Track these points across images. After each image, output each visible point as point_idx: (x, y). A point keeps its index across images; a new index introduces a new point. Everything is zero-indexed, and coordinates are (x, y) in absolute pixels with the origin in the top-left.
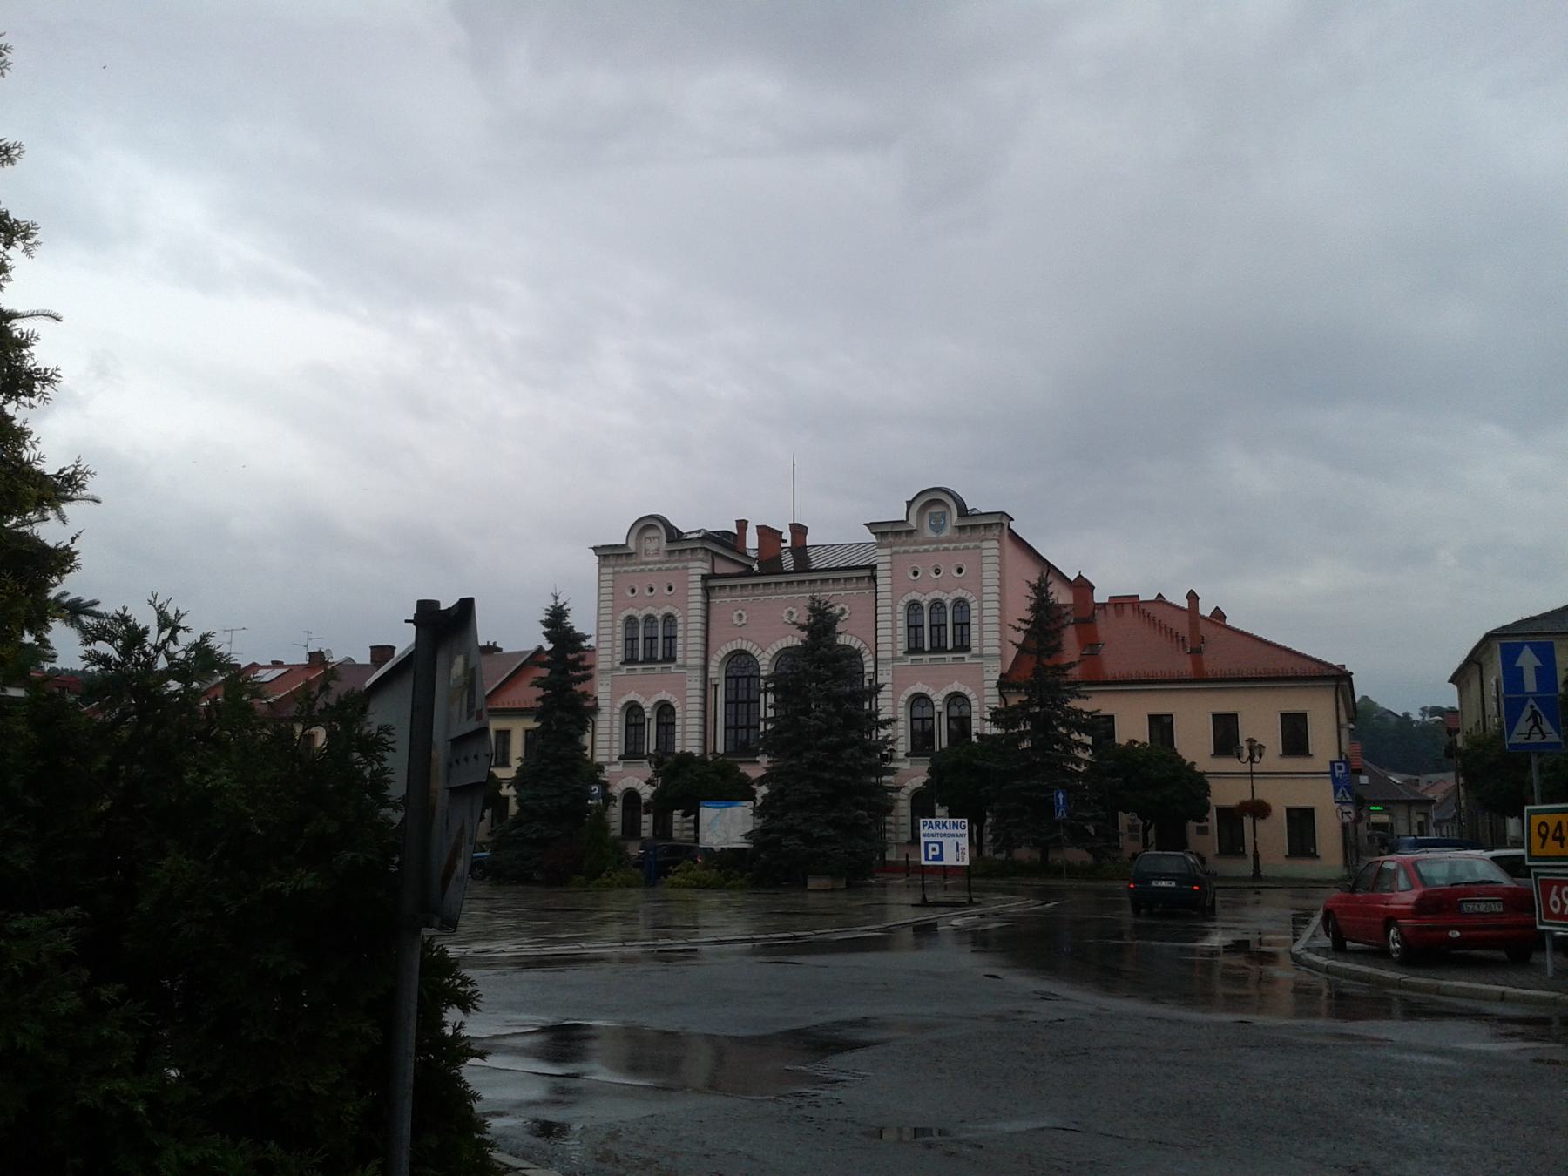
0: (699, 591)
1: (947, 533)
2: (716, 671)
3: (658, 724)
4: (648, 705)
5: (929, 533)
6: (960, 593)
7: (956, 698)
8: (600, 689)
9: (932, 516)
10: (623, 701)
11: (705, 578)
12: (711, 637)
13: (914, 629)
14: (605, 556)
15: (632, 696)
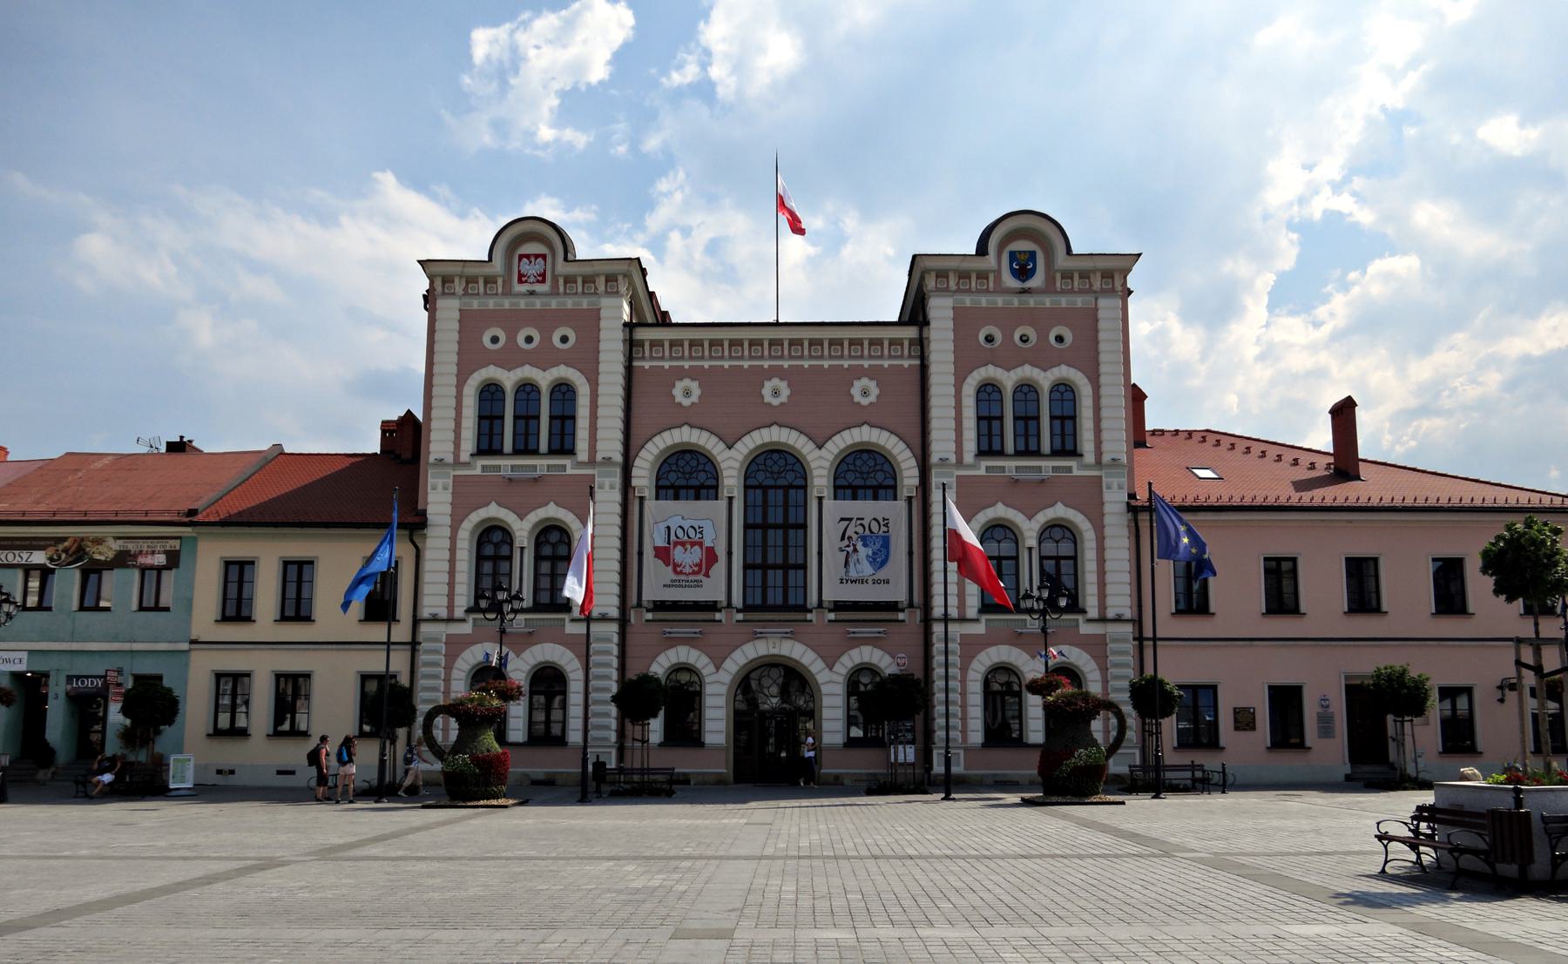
0: (620, 346)
1: (1037, 281)
2: (643, 477)
3: (538, 558)
4: (522, 530)
5: (1010, 282)
6: (1064, 372)
7: (1058, 530)
8: (431, 498)
9: (1013, 255)
10: (476, 517)
11: (629, 326)
12: (634, 421)
13: (988, 421)
14: (447, 280)
15: (493, 511)
